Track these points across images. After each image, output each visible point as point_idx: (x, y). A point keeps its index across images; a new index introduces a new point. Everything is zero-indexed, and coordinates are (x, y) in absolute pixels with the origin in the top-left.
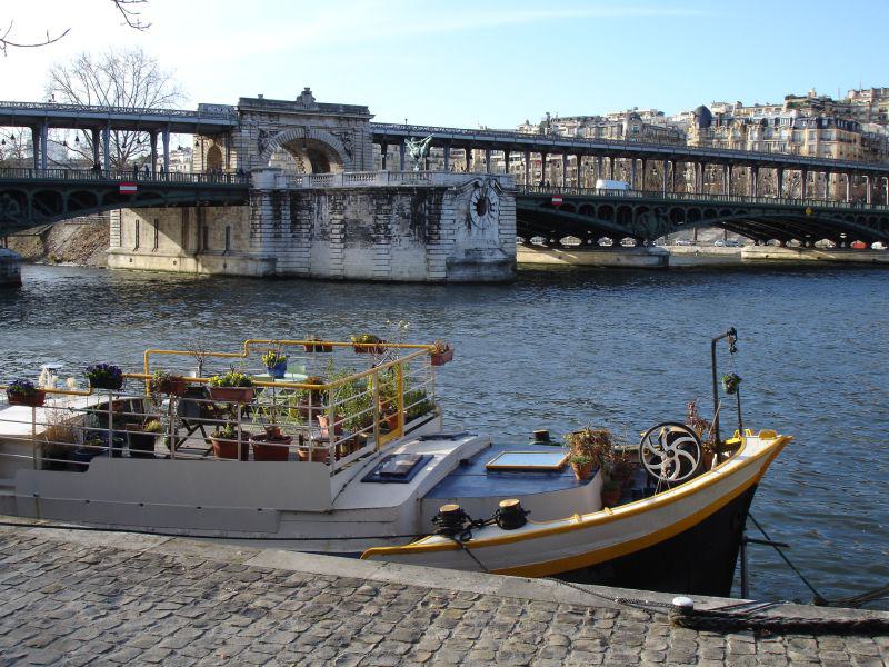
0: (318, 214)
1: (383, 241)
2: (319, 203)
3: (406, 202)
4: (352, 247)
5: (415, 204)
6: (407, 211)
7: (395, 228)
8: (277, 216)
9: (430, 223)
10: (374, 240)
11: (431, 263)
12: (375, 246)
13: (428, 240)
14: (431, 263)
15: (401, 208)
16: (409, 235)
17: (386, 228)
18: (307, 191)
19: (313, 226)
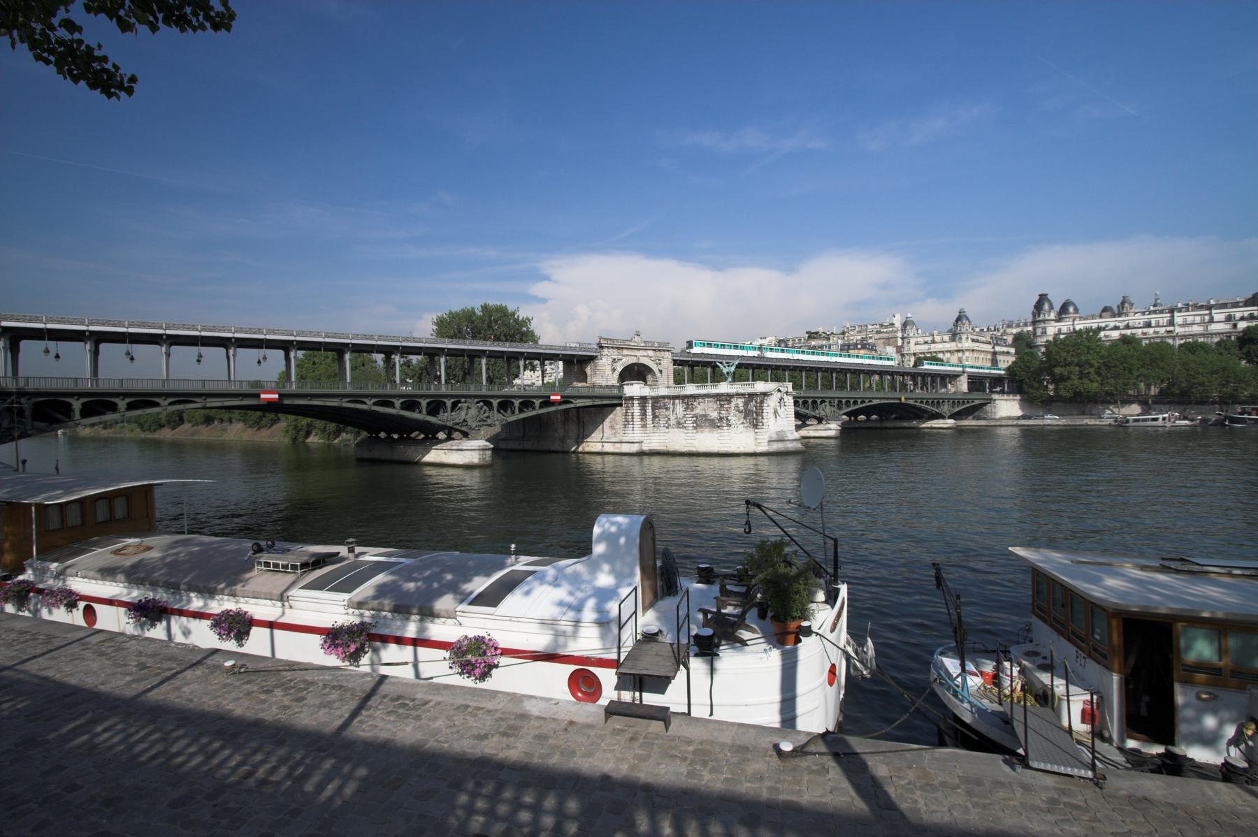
0: (673, 411)
1: (725, 428)
2: (674, 404)
3: (740, 402)
4: (702, 432)
5: (746, 404)
6: (742, 408)
7: (732, 419)
8: (644, 413)
9: (757, 415)
10: (718, 427)
11: (759, 441)
12: (719, 431)
13: (756, 426)
14: (759, 441)
15: (737, 406)
16: (743, 423)
17: (727, 419)
18: (664, 397)
19: (669, 419)
